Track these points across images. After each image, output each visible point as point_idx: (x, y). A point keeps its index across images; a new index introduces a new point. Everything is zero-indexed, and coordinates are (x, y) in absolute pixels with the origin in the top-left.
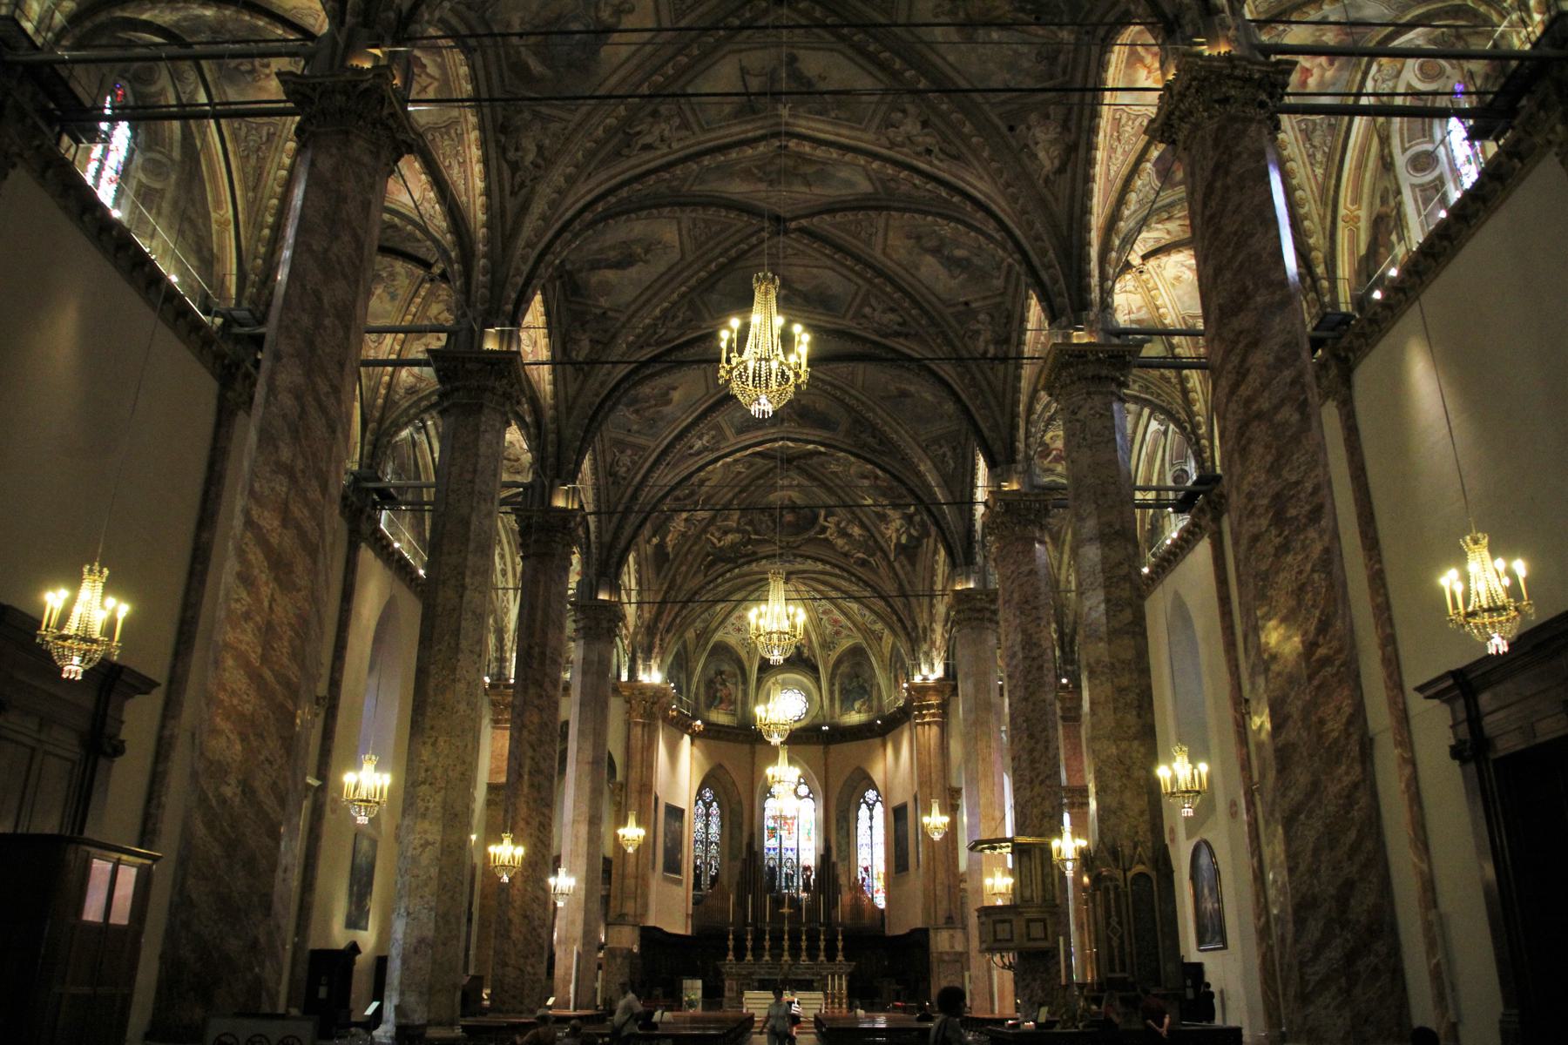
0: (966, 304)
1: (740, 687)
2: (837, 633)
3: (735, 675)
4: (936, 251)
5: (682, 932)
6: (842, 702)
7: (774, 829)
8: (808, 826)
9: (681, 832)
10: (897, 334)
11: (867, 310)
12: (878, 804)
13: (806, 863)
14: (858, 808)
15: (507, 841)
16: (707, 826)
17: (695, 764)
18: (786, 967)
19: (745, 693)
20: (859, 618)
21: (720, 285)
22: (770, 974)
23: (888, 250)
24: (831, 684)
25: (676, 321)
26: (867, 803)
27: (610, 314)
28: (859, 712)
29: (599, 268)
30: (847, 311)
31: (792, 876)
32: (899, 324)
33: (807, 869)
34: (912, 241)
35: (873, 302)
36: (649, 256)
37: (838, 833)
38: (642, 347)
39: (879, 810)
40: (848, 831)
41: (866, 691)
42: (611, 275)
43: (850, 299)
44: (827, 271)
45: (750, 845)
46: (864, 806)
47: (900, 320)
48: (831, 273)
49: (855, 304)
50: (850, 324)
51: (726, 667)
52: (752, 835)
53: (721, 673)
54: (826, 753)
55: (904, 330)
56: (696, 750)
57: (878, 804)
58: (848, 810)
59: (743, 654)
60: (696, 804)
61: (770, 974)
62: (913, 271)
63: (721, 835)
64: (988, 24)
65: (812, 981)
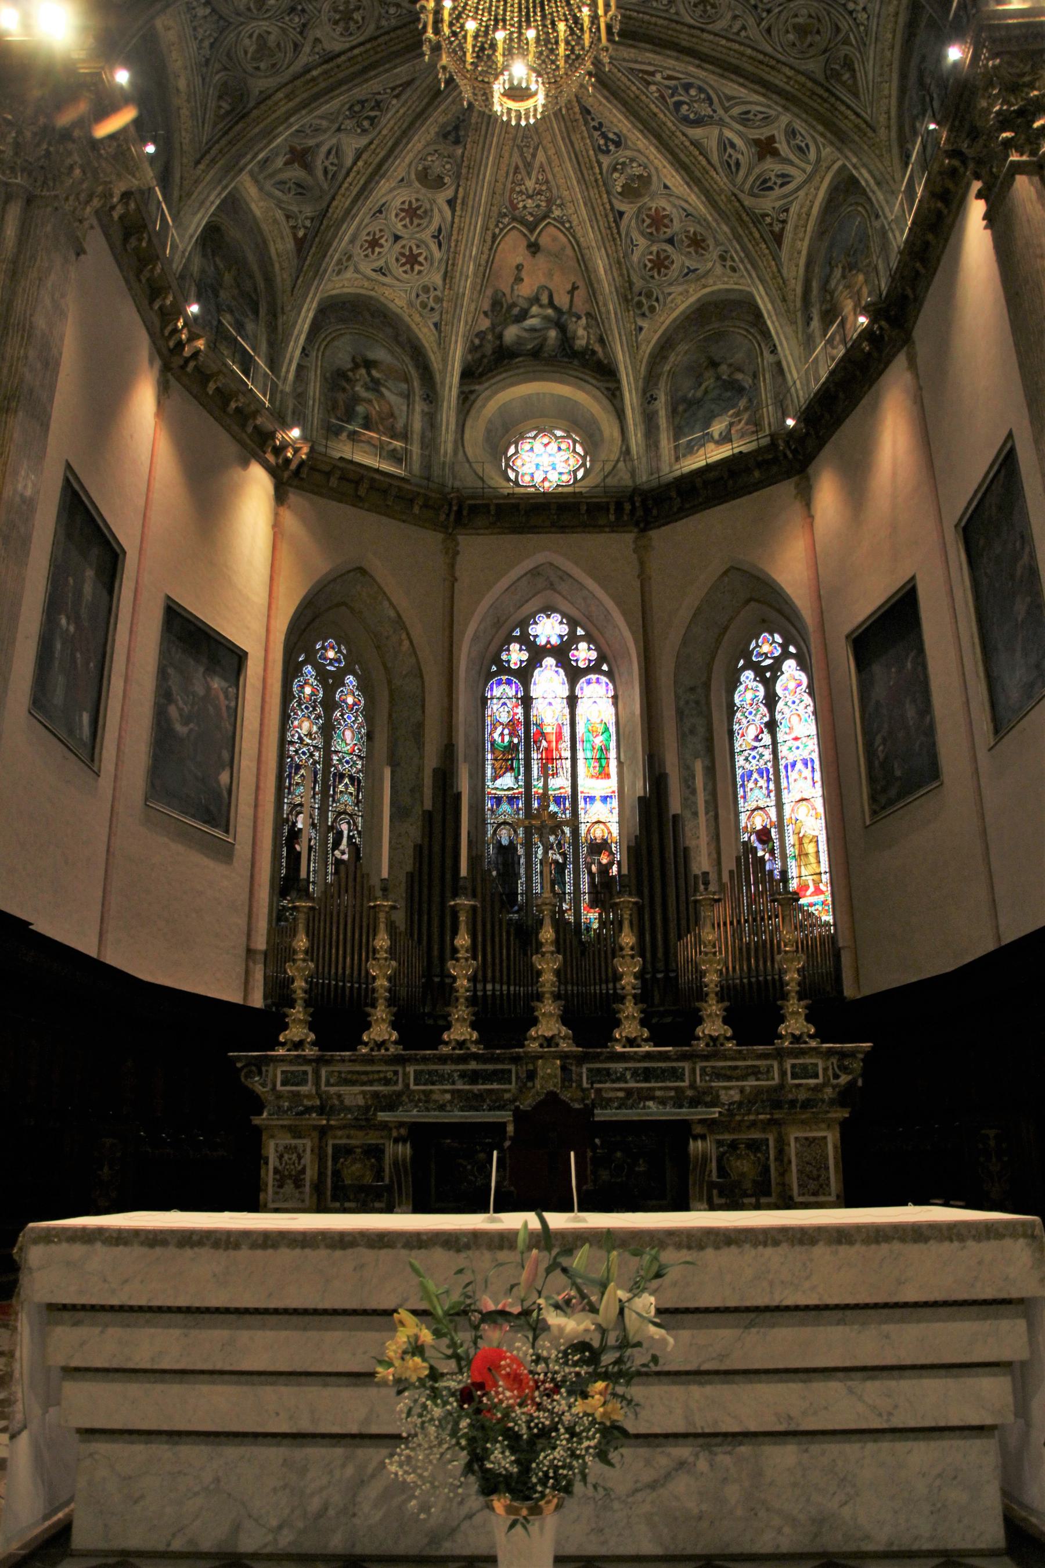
1: (419, 407)
2: (660, 263)
3: (407, 380)
5: (234, 996)
6: (678, 432)
7: (512, 748)
8: (598, 741)
9: (234, 713)
12: (790, 666)
13: (598, 832)
14: (734, 683)
16: (328, 730)
17: (284, 548)
18: (549, 1072)
19: (432, 421)
20: (721, 180)
22: (473, 1101)
24: (648, 398)
26: (759, 672)
28: (726, 438)
31: (561, 868)
33: (598, 847)
37: (682, 738)
39: (791, 674)
40: (709, 741)
41: (740, 390)
45: (445, 777)
46: (748, 676)
51: (379, 354)
52: (448, 752)
53: (369, 364)
54: (641, 550)
56: (289, 518)
57: (790, 666)
58: (707, 685)
59: (426, 335)
60: (291, 671)
61: (473, 1101)
63: (368, 758)
65: (682, 1130)
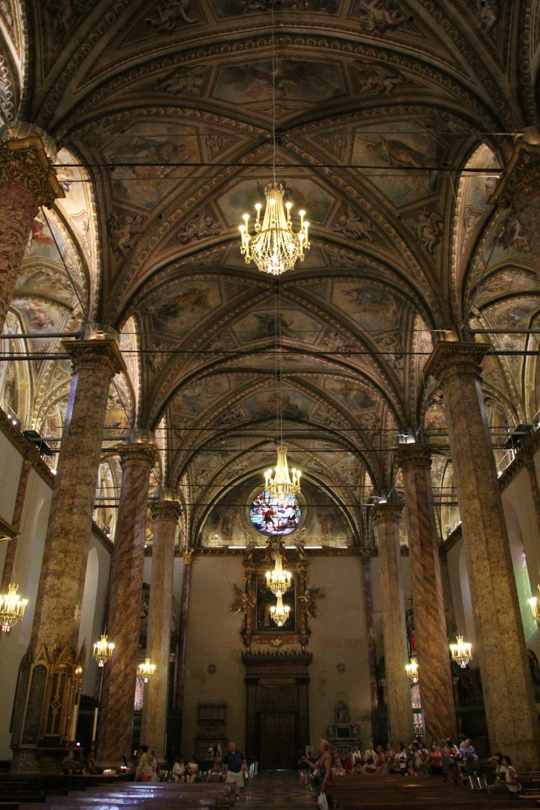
0: (123, 132)
4: (159, 147)
10: (169, 77)
11: (199, 82)
15: (460, 640)
21: (330, 94)
23: (194, 131)
25: (374, 82)
27: (424, 125)
29: (417, 152)
30: (217, 73)
32: (169, 86)
34: (179, 145)
35: (196, 90)
36: (380, 140)
38: (410, 82)
42: (411, 143)
43: (217, 87)
44: (239, 102)
47: (169, 89)
48: (237, 101)
49: (211, 80)
50: (215, 63)
55: (163, 85)
62: (171, 126)
64: (185, 295)
